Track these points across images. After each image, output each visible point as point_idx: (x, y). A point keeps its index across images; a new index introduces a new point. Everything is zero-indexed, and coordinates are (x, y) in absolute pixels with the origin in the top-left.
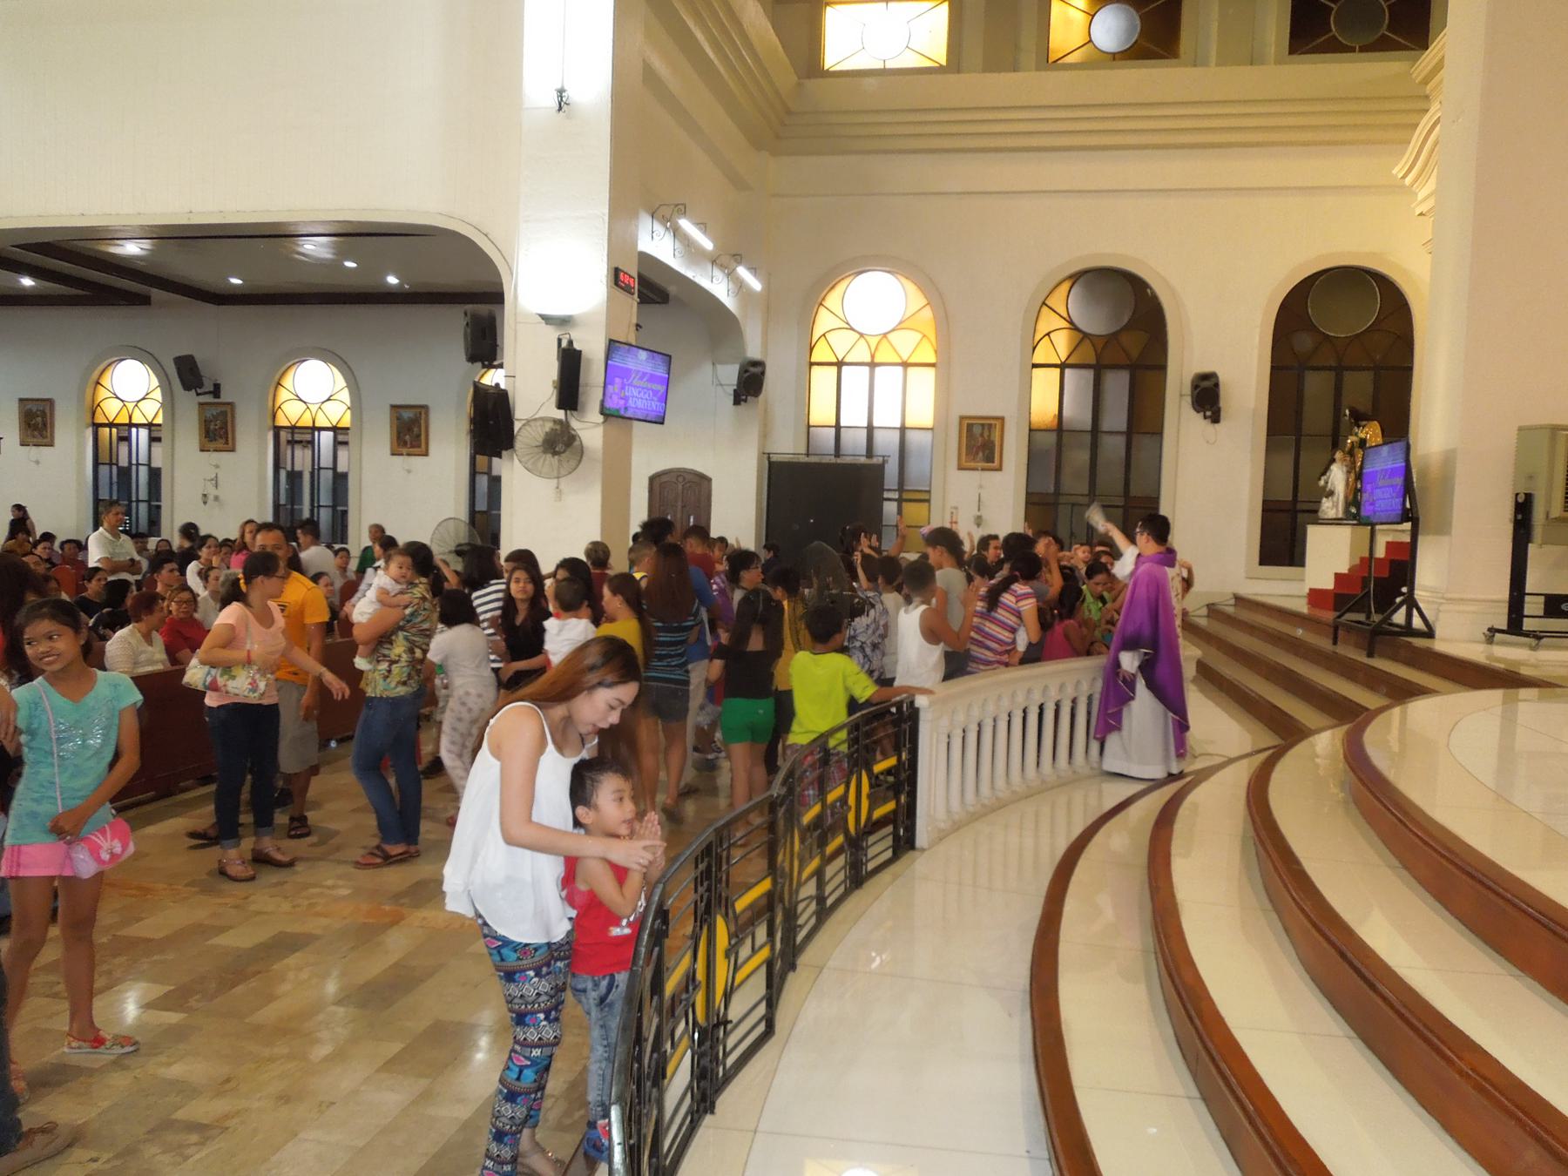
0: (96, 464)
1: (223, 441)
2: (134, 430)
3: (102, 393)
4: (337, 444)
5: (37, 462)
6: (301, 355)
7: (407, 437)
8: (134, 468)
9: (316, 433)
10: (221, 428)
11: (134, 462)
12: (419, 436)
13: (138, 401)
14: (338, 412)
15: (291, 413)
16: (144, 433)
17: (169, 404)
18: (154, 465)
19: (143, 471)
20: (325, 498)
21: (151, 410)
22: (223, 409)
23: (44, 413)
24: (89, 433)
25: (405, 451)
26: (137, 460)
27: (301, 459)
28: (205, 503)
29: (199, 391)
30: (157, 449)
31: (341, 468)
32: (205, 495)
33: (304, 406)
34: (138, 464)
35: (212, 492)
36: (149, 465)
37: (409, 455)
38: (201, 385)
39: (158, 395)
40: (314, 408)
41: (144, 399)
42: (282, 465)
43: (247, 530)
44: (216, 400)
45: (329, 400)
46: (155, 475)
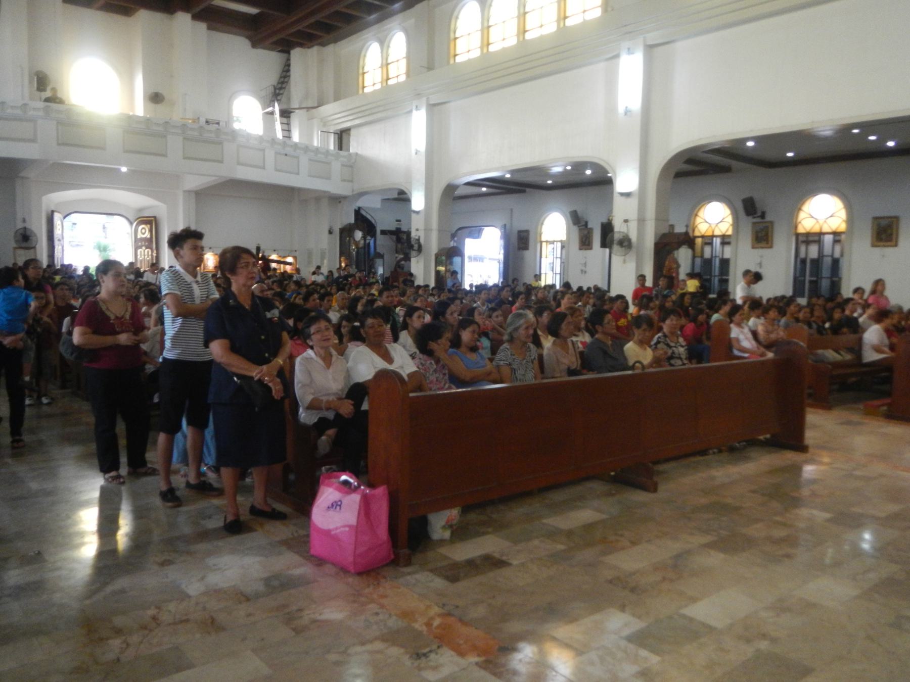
2: (714, 239)
4: (836, 241)
8: (714, 259)
11: (714, 255)
12: (891, 234)
13: (718, 224)
17: (736, 224)
22: (767, 224)
25: (881, 244)
29: (755, 216)
31: (837, 254)
38: (755, 213)
41: (721, 222)
45: (831, 216)
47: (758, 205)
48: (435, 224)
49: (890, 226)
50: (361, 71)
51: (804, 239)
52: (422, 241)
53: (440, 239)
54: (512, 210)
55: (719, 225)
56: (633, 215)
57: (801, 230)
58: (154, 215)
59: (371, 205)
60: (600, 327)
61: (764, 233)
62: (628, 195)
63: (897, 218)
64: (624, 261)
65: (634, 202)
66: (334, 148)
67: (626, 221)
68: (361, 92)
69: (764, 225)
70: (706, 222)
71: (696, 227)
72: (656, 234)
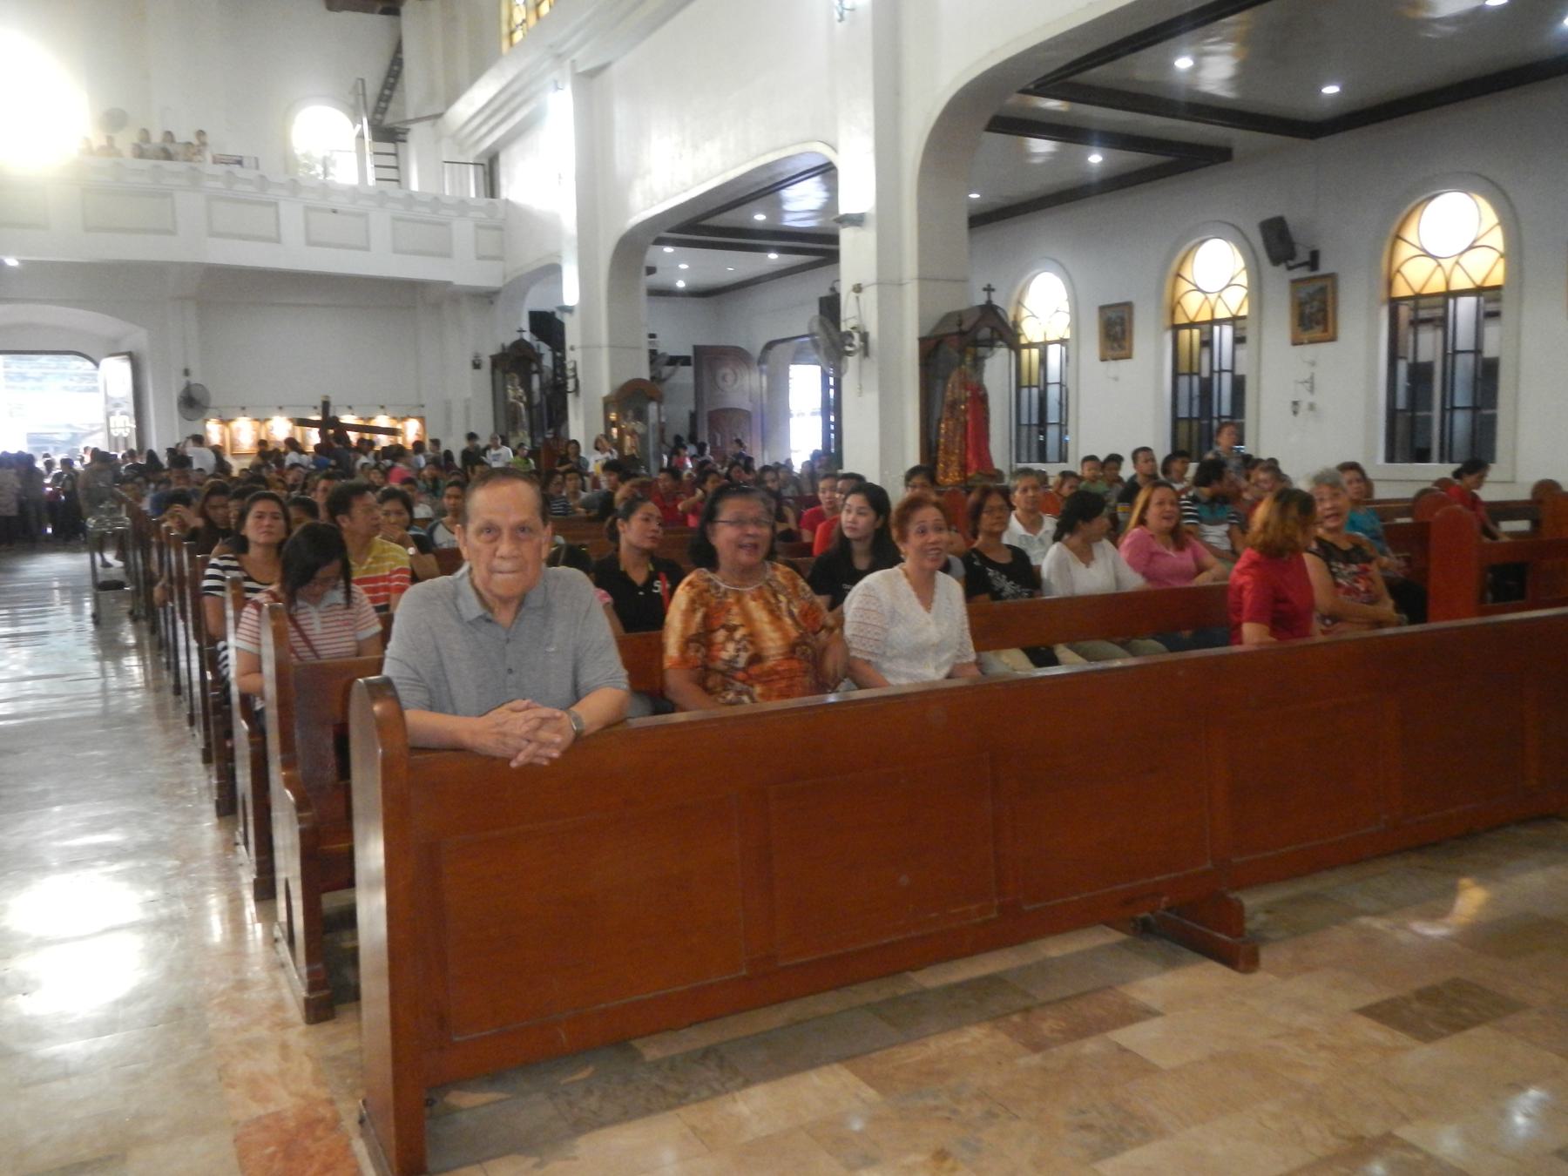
0: (1176, 374)
1: (1320, 328)
2: (1216, 329)
3: (1184, 286)
5: (1116, 379)
6: (1426, 190)
9: (1451, 302)
11: (1216, 368)
13: (1221, 291)
15: (1416, 275)
16: (1228, 332)
18: (1239, 372)
19: (1227, 379)
20: (1462, 397)
21: (1235, 301)
23: (1122, 319)
24: (1168, 336)
26: (1220, 364)
27: (1428, 345)
28: (1295, 413)
29: (1291, 263)
30: (1242, 352)
31: (1489, 351)
32: (1295, 403)
33: (1432, 263)
34: (1221, 371)
35: (1305, 398)
36: (1232, 371)
39: (1243, 279)
40: (1447, 264)
41: (1228, 286)
42: (1401, 354)
45: (1471, 247)
46: (1239, 384)
47: (1298, 235)
48: (603, 337)
53: (613, 363)
55: (1224, 295)
57: (1402, 290)
58: (129, 350)
61: (1316, 304)
66: (477, 194)
69: (1319, 284)
70: (1199, 290)
71: (1179, 303)
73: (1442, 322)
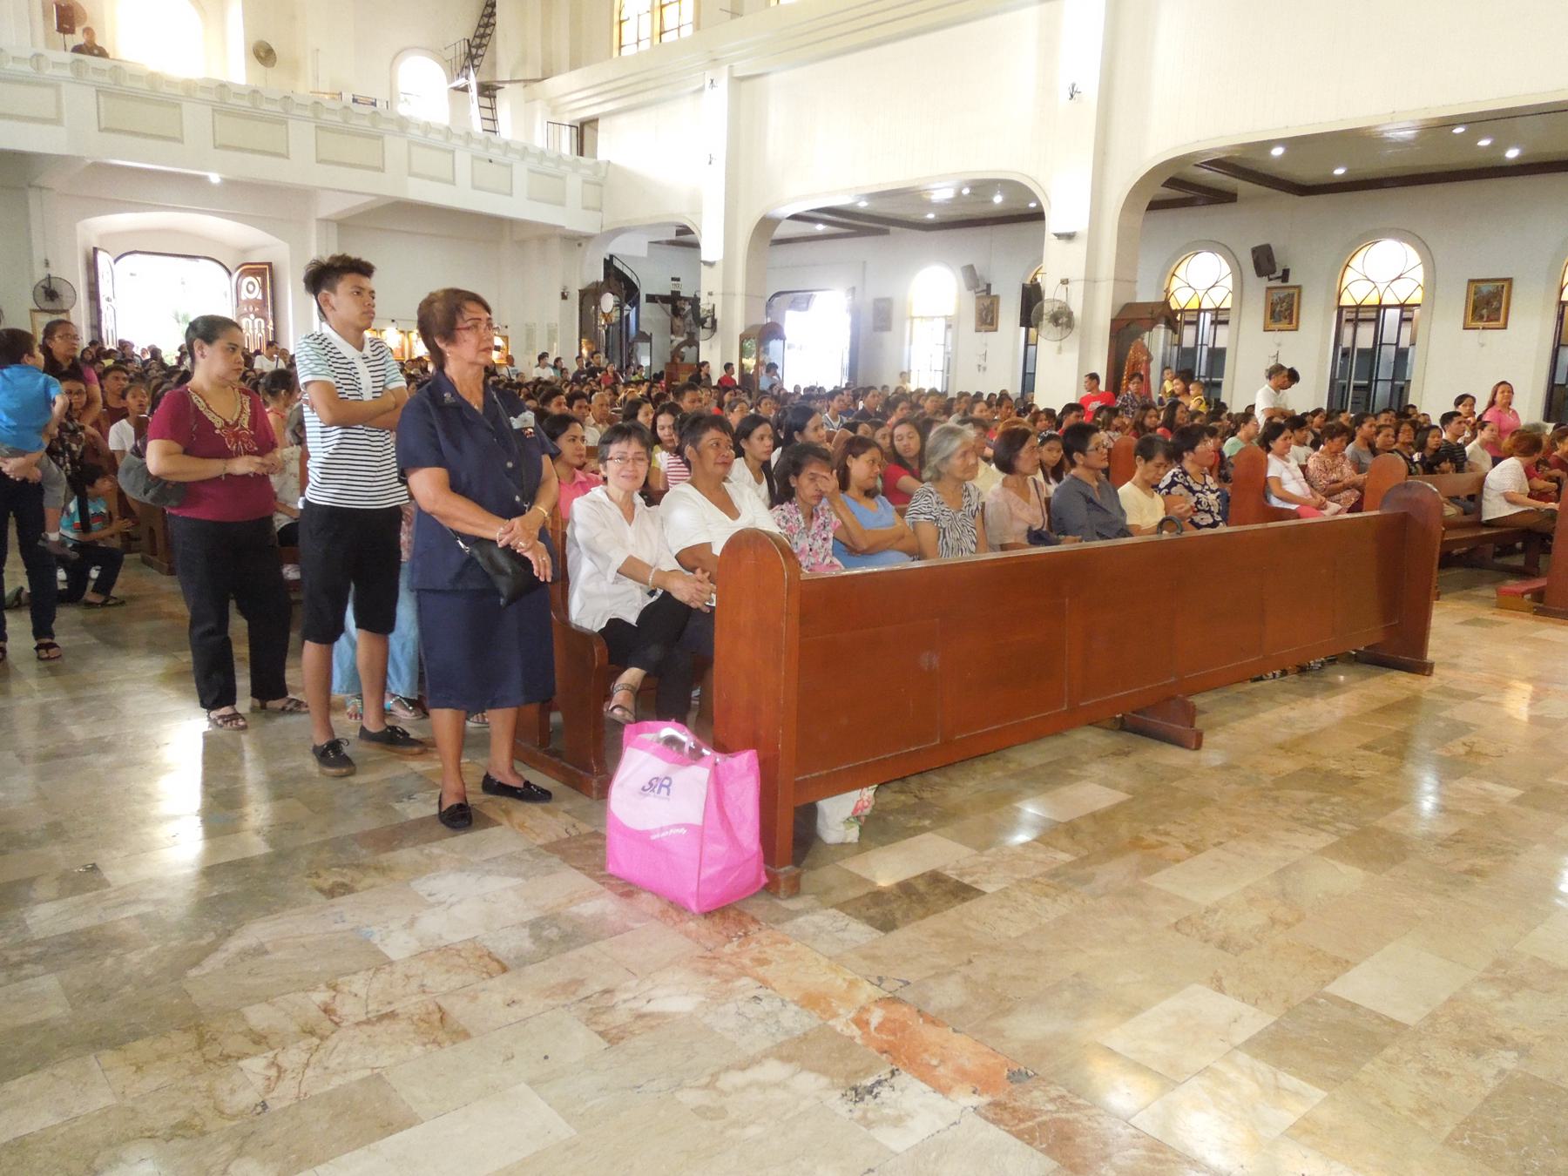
1: (1287, 321)
2: (1202, 314)
6: (1371, 237)
7: (1485, 311)
10: (1286, 310)
11: (1200, 343)
12: (1498, 309)
14: (1410, 289)
15: (1356, 292)
16: (1208, 316)
22: (1291, 291)
25: (1481, 324)
29: (1271, 276)
31: (1404, 343)
37: (1483, 328)
41: (1213, 286)
43: (1500, 390)
44: (1284, 284)
45: (1399, 278)
47: (1278, 258)
49: (1497, 295)
50: (616, 18)
51: (1352, 316)
52: (718, 316)
53: (748, 312)
54: (864, 262)
56: (1077, 271)
57: (1347, 300)
59: (632, 252)
60: (1081, 456)
62: (1070, 237)
63: (1509, 281)
64: (1060, 350)
65: (1078, 249)
67: (1065, 282)
68: (616, 53)
69: (1286, 292)
72: (1113, 306)
73: (1377, 321)
